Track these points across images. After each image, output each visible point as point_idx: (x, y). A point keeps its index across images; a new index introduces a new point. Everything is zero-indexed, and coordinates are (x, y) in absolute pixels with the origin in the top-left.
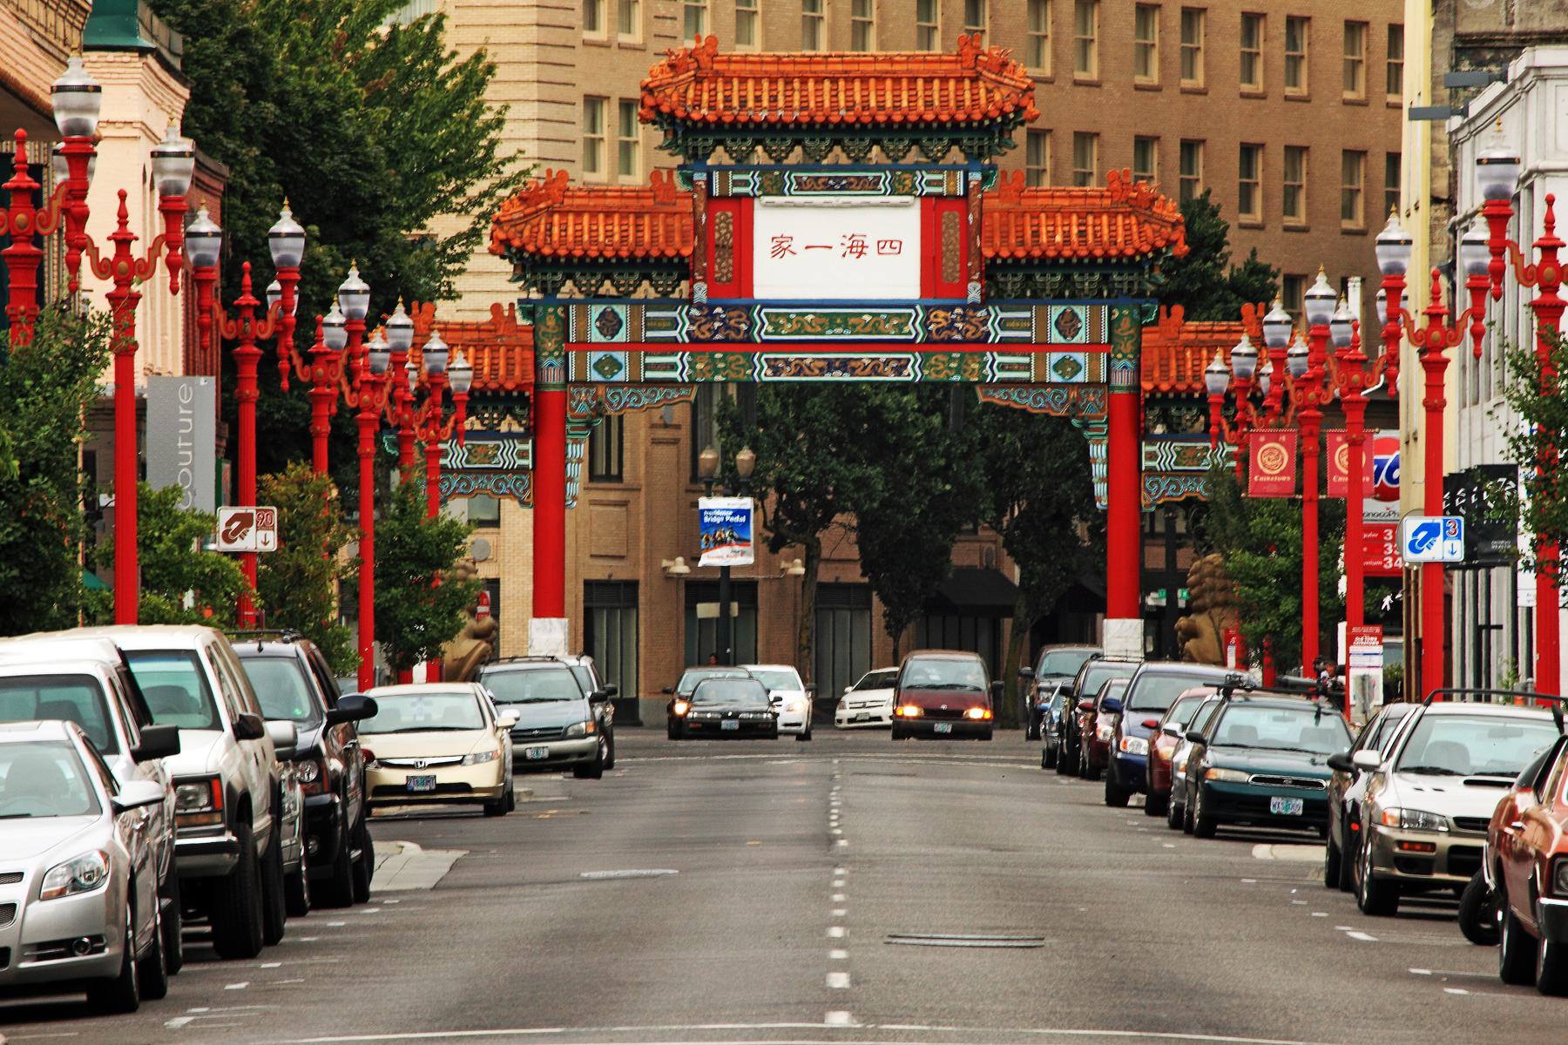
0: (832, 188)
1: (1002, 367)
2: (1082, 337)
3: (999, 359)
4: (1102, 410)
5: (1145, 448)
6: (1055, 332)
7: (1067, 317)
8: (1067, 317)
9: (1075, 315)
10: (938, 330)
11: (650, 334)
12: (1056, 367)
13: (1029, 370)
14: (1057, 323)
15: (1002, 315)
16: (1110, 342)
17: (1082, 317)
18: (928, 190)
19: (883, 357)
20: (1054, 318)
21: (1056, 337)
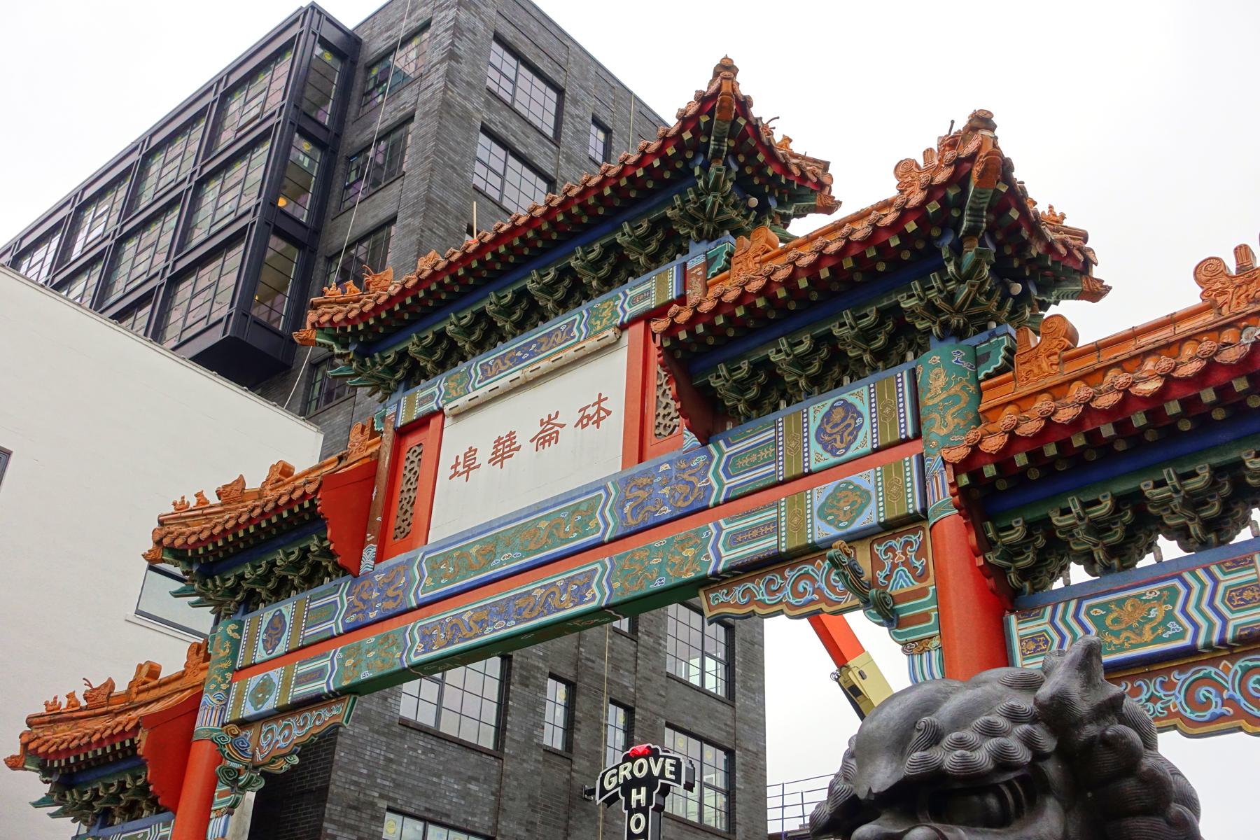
0: (521, 360)
1: (735, 540)
2: (863, 442)
3: (728, 528)
4: (922, 577)
5: (1018, 628)
6: (815, 447)
7: (837, 416)
8: (837, 416)
9: (849, 408)
10: (634, 509)
11: (308, 632)
12: (822, 514)
13: (777, 531)
14: (820, 430)
15: (729, 451)
16: (918, 435)
17: (863, 408)
18: (632, 311)
19: (559, 579)
20: (813, 427)
21: (817, 457)
